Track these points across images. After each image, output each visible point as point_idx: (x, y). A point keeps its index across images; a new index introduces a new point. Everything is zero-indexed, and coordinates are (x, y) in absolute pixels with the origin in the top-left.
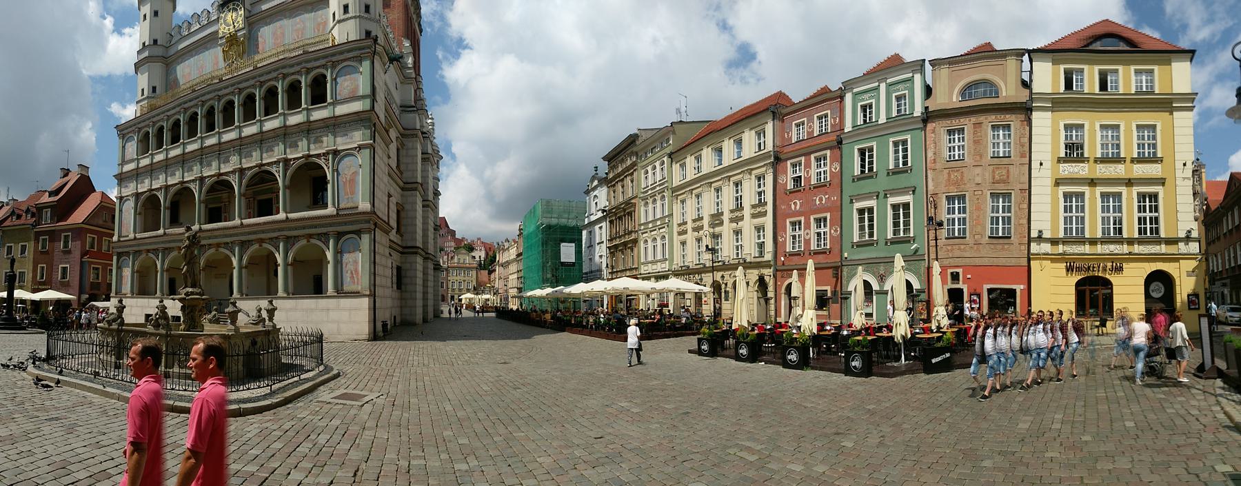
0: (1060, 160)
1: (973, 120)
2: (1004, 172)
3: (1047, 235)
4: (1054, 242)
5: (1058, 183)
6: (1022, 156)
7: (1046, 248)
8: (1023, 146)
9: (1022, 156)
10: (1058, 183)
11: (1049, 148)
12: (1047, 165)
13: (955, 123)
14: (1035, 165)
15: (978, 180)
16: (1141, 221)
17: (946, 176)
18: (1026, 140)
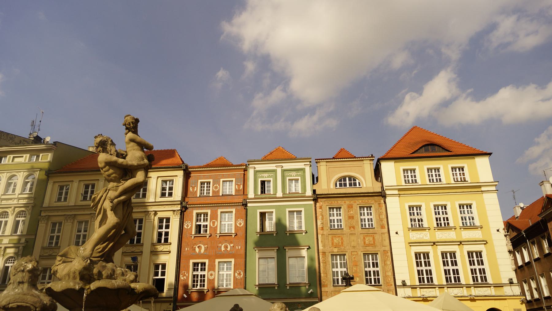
1: (347, 202)
2: (371, 239)
3: (408, 283)
4: (413, 287)
8: (382, 220)
9: (382, 227)
12: (401, 233)
13: (335, 203)
15: (353, 244)
17: (330, 239)
18: (384, 216)
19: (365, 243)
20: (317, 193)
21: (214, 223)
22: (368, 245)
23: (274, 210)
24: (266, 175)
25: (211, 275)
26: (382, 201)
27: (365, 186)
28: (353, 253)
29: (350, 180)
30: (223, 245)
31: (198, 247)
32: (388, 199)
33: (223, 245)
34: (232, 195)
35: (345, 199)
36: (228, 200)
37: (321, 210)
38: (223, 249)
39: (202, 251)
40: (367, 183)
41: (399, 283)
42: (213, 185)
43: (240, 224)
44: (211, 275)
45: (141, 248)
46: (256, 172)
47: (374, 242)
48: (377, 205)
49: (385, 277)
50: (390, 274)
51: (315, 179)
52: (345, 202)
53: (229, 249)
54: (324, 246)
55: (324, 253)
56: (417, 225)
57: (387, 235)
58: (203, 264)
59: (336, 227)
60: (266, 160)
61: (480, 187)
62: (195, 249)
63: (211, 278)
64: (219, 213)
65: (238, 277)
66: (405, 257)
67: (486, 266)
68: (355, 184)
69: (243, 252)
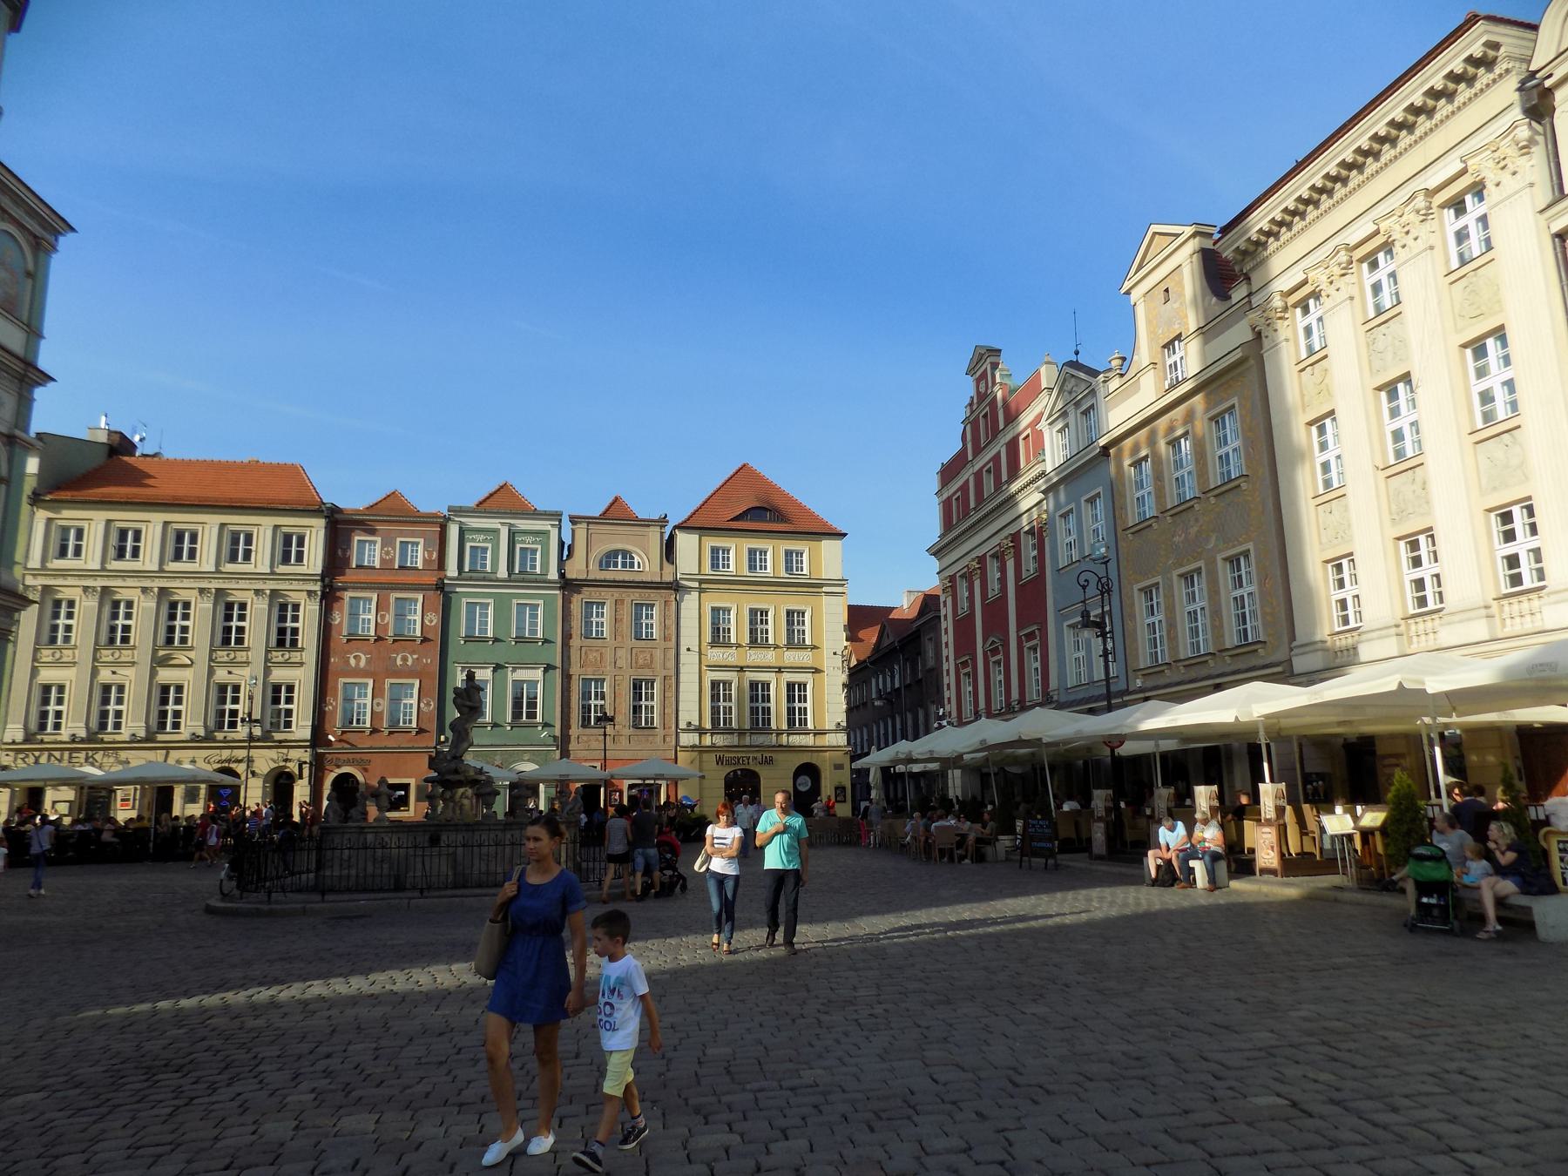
4: (701, 731)
18: (671, 622)
21: (383, 617)
23: (491, 601)
29: (624, 557)
38: (399, 662)
39: (362, 664)
40: (647, 563)
41: (682, 725)
49: (663, 714)
53: (410, 663)
56: (719, 637)
61: (821, 586)
64: (392, 600)
67: (809, 705)
68: (632, 565)
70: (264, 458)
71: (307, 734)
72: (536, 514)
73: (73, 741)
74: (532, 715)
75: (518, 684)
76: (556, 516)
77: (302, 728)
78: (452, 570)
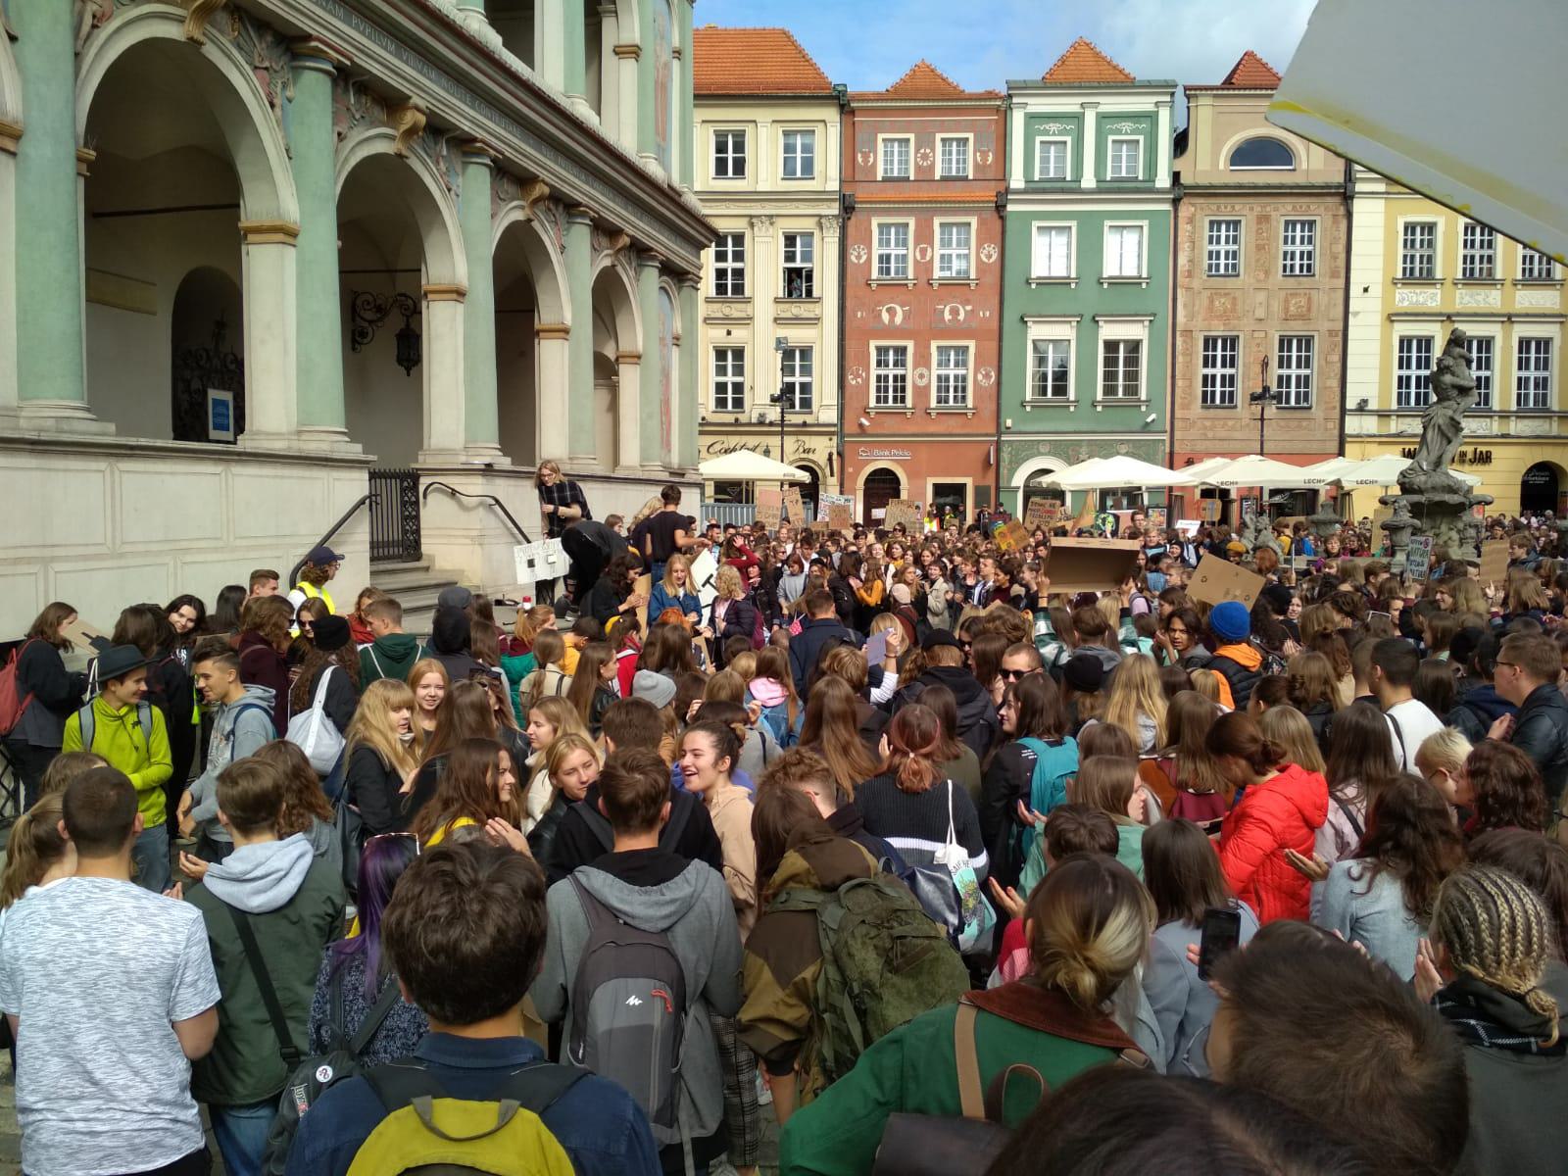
0: (1395, 282)
3: (1373, 405)
4: (1383, 415)
5: (1391, 318)
6: (1334, 275)
7: (1370, 425)
8: (1335, 258)
9: (1334, 275)
10: (1391, 318)
11: (1379, 263)
13: (1227, 209)
14: (1355, 290)
15: (1260, 313)
16: (1522, 383)
17: (1206, 302)
18: (1341, 248)
19: (1287, 309)
20: (1184, 180)
21: (923, 252)
22: (1295, 318)
23: (1073, 224)
24: (1054, 127)
25: (922, 376)
26: (1342, 210)
27: (1304, 166)
28: (1256, 335)
30: (948, 308)
31: (888, 310)
32: (1359, 206)
33: (948, 308)
34: (965, 179)
35: (1251, 200)
36: (955, 191)
37: (1189, 227)
38: (947, 316)
39: (898, 319)
42: (917, 151)
43: (989, 256)
44: (922, 376)
45: (749, 307)
46: (1031, 118)
47: (1309, 310)
48: (1329, 221)
49: (1323, 389)
50: (1335, 383)
51: (1181, 143)
52: (1252, 209)
53: (961, 317)
54: (1191, 316)
55: (1188, 333)
57: (1340, 294)
58: (901, 351)
59: (1222, 271)
60: (1051, 84)
62: (880, 315)
63: (922, 383)
65: (984, 383)
66: (1376, 347)
69: (995, 325)
70: (721, 25)
71: (830, 416)
72: (1124, 84)
73: (761, 423)
74: (1132, 390)
75: (1111, 346)
76: (1167, 87)
77: (825, 409)
78: (1017, 181)
